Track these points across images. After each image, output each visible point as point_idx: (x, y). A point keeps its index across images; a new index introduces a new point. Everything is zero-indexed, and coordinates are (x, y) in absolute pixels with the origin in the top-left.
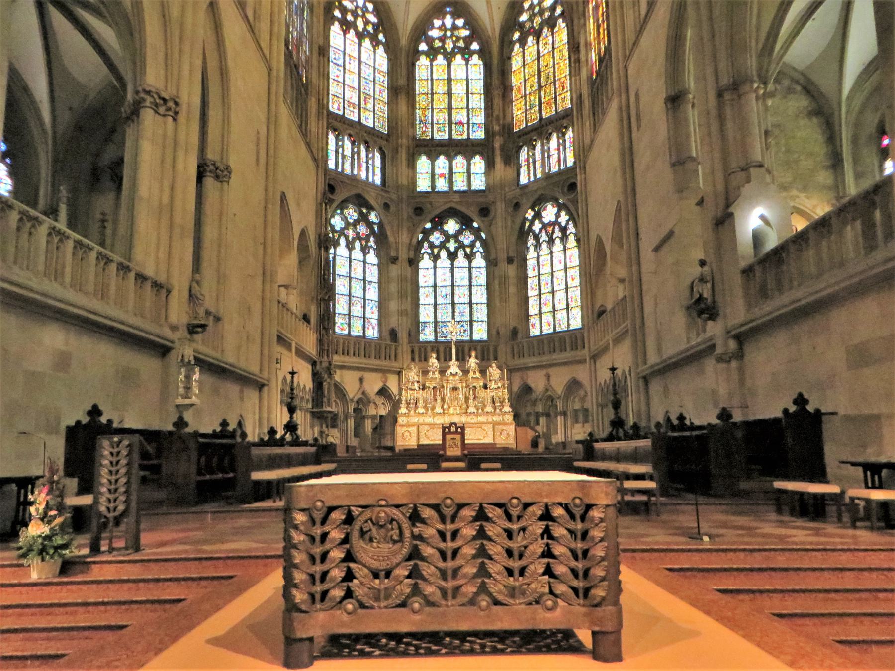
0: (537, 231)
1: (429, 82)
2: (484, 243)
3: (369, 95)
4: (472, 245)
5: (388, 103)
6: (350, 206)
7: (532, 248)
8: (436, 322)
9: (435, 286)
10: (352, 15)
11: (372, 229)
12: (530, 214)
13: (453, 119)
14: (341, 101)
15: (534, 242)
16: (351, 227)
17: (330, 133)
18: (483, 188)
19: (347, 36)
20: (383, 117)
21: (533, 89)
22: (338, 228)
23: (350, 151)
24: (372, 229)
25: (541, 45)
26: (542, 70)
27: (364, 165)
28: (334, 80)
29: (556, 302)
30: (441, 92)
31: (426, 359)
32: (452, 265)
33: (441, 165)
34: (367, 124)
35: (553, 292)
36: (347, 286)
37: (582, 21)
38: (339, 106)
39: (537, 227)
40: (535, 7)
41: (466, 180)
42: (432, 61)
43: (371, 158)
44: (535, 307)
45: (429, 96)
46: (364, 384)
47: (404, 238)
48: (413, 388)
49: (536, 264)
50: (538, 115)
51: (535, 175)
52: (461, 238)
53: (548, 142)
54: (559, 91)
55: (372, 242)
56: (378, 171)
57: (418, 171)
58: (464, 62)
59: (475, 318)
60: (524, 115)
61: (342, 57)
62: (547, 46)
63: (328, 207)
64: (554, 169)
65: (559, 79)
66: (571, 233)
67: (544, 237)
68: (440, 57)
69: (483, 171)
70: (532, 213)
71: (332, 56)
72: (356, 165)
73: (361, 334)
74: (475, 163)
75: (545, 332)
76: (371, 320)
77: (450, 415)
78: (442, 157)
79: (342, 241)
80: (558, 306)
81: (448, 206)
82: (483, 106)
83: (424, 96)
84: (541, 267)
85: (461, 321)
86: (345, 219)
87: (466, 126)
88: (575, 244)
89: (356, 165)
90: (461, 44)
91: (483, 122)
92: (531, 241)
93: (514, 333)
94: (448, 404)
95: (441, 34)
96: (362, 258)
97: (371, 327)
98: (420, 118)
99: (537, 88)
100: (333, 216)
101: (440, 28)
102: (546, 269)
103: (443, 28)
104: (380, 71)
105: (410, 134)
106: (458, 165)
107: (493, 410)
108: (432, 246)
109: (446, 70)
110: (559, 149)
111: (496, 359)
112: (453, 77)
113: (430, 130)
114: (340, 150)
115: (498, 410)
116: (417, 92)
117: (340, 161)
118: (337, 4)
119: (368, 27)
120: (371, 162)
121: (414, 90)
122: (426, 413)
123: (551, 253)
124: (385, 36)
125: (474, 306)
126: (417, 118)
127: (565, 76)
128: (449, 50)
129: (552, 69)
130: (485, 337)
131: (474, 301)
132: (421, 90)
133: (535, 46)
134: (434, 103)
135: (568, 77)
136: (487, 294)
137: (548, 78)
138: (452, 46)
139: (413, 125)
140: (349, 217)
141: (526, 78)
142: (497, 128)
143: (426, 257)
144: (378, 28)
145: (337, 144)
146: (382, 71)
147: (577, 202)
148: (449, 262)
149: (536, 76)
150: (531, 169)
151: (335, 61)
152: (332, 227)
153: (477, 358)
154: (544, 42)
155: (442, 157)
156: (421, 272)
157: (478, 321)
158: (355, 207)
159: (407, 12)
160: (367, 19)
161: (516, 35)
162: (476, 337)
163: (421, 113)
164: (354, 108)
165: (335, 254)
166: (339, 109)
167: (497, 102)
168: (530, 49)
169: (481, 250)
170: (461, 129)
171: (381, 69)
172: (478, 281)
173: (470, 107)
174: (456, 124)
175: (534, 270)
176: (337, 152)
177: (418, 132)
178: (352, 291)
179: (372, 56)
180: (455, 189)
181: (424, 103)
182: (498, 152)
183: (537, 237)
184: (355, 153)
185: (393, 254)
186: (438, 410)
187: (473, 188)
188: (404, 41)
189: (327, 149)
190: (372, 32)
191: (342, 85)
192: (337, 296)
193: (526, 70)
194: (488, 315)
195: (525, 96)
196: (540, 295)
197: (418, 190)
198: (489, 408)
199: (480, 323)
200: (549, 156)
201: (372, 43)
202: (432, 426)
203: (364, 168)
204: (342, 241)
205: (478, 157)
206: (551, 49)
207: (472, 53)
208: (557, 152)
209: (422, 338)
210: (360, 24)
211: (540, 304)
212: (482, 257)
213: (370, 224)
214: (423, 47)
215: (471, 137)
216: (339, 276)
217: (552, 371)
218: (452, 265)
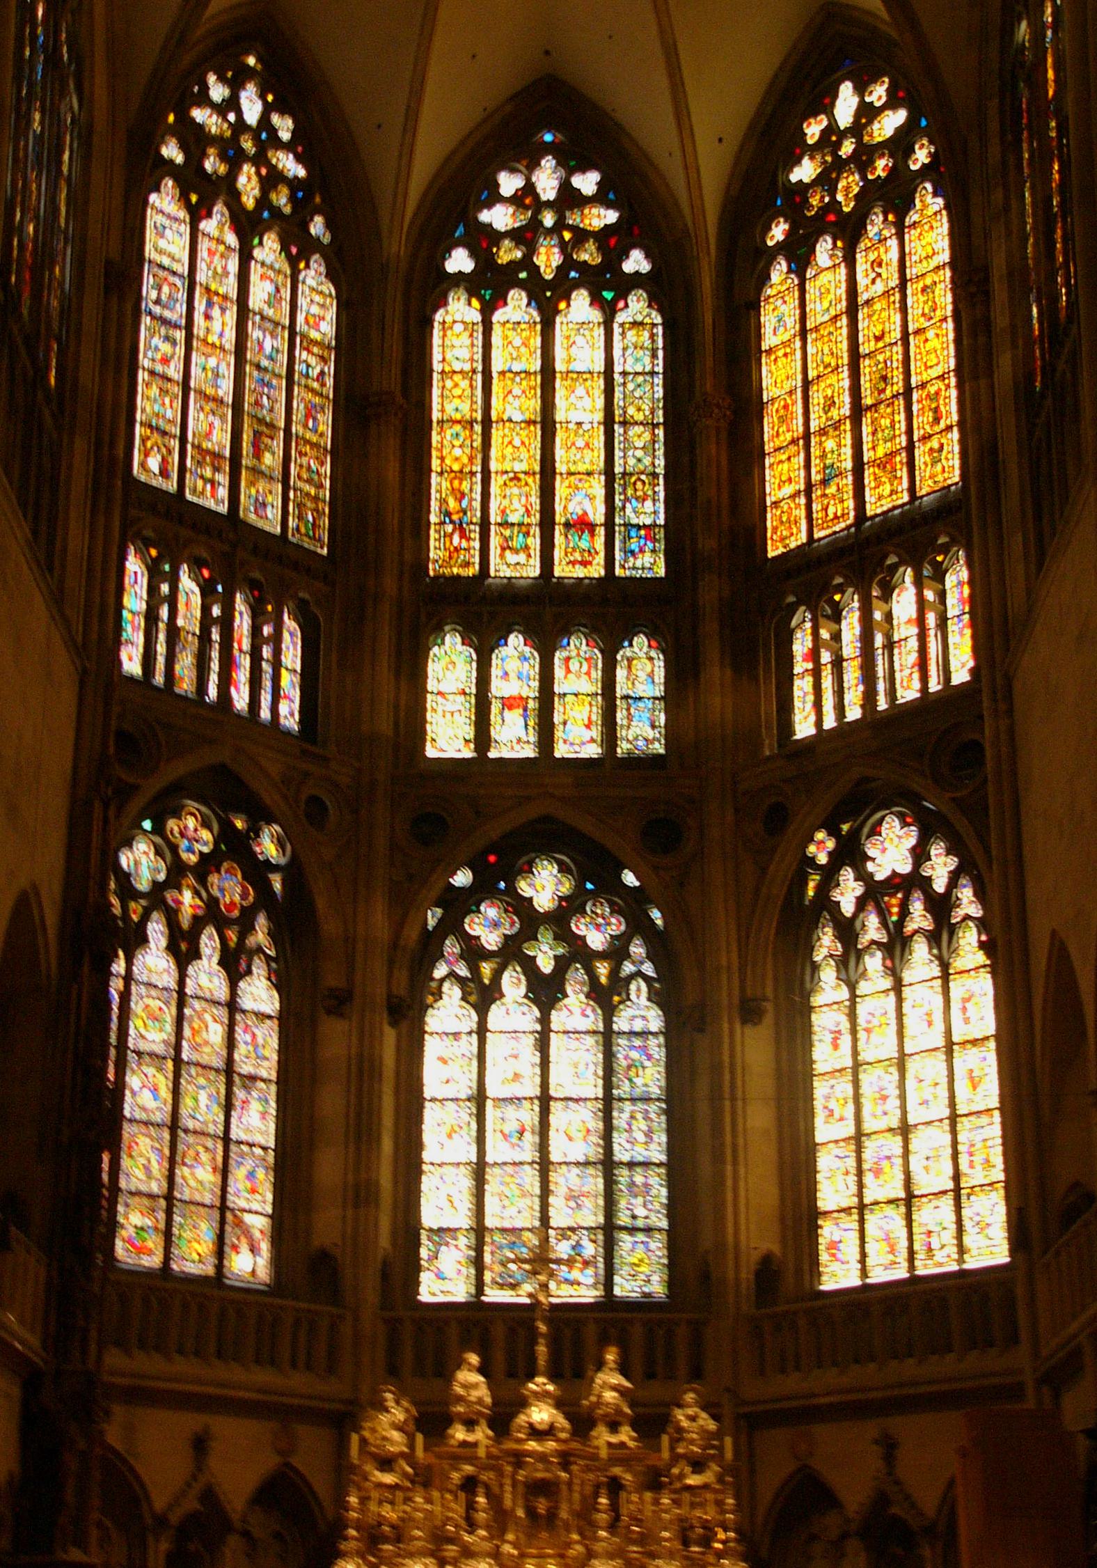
0: (848, 908)
1: (479, 377)
2: (659, 947)
3: (271, 426)
4: (616, 952)
5: (334, 453)
6: (192, 805)
7: (828, 974)
8: (480, 1231)
9: (479, 1099)
10: (223, 157)
11: (263, 888)
12: (821, 848)
13: (558, 508)
14: (175, 444)
15: (839, 949)
16: (191, 880)
17: (132, 550)
18: (659, 748)
19: (204, 225)
20: (316, 499)
21: (834, 413)
22: (143, 883)
23: (198, 614)
24: (263, 888)
25: (861, 266)
26: (864, 349)
27: (246, 662)
28: (152, 373)
29: (915, 1164)
30: (517, 417)
31: (445, 1372)
32: (545, 1020)
33: (513, 665)
34: (260, 524)
36: (165, 1093)
37: (998, 196)
38: (164, 461)
39: (848, 893)
40: (843, 135)
41: (596, 717)
42: (487, 311)
43: (267, 641)
44: (840, 1178)
45: (478, 428)
46: (214, 1463)
47: (379, 921)
49: (845, 1025)
50: (850, 504)
51: (840, 708)
52: (580, 927)
53: (887, 596)
54: (922, 422)
55: (260, 936)
56: (290, 683)
57: (431, 685)
58: (596, 316)
59: (623, 1219)
60: (802, 500)
61: (182, 296)
62: (882, 271)
63: (112, 813)
64: (908, 693)
65: (923, 386)
66: (967, 917)
67: (872, 930)
68: (517, 299)
69: (659, 691)
70: (831, 844)
71: (149, 292)
72: (215, 666)
73: (210, 1270)
74: (630, 660)
75: (878, 1276)
76: (248, 1219)
78: (516, 640)
79: (156, 930)
80: (923, 1184)
81: (533, 811)
82: (660, 470)
83: (458, 428)
84: (862, 1035)
86: (167, 849)
87: (601, 531)
88: (981, 958)
89: (215, 666)
90: (589, 255)
91: (661, 521)
92: (826, 942)
93: (767, 1272)
95: (523, 219)
96: (222, 993)
97: (244, 1248)
98: (443, 501)
99: (846, 410)
100: (128, 843)
101: (517, 200)
102: (879, 1045)
103: (526, 198)
104: (309, 344)
105: (408, 556)
106: (574, 665)
108: (473, 952)
109: (537, 341)
110: (921, 621)
111: (696, 1374)
112: (560, 366)
113: (477, 544)
114: (164, 612)
116: (436, 415)
117: (161, 648)
118: (171, 118)
119: (273, 196)
120: (266, 652)
121: (424, 406)
123: (898, 987)
124: (328, 225)
125: (623, 1175)
126: (434, 505)
127: (941, 377)
128: (549, 276)
129: (899, 349)
130: (657, 1288)
131: (621, 1154)
132: (449, 408)
133: (843, 271)
134: (494, 453)
135: (953, 381)
136: (670, 1132)
137: (884, 378)
138: (556, 259)
139: (420, 528)
140: (184, 844)
141: (812, 374)
142: (708, 544)
143: (452, 993)
144: (309, 197)
145: (152, 590)
146: (316, 343)
147: (986, 809)
148: (537, 1013)
149: (845, 374)
150: (827, 682)
151: (157, 310)
152: (125, 879)
153: (624, 1370)
154: (872, 256)
155: (516, 640)
156: (432, 1048)
157: (632, 1230)
158: (204, 809)
159: (407, 152)
160: (273, 169)
161: (778, 232)
162: (625, 1288)
163: (445, 485)
164: (216, 469)
165: (128, 978)
166: (164, 473)
167: (713, 452)
168: (825, 278)
169: (648, 969)
170: (584, 544)
171: (314, 335)
172: (639, 1081)
173: (618, 469)
174: (567, 525)
175: (836, 1046)
176: (151, 617)
177: (436, 552)
178: (184, 1112)
179: (286, 294)
180: (561, 751)
181: (457, 452)
182: (710, 627)
183: (847, 931)
184: (216, 621)
185: (332, 979)
187: (623, 748)
188: (396, 245)
189: (120, 606)
190: (287, 210)
191: (177, 390)
192: (126, 1125)
193: (811, 350)
194: (672, 1209)
195: (807, 436)
196: (858, 1139)
197: (431, 752)
199: (641, 1237)
200: (890, 646)
201: (285, 248)
203: (242, 676)
204: (156, 930)
205: (640, 641)
206: (894, 282)
207: (625, 285)
208: (914, 630)
209: (430, 1290)
210: (248, 183)
211: (860, 1173)
212: (655, 997)
213: (256, 871)
214: (460, 261)
215: (619, 572)
216: (139, 1053)
217: (898, 1424)
218: (545, 1020)
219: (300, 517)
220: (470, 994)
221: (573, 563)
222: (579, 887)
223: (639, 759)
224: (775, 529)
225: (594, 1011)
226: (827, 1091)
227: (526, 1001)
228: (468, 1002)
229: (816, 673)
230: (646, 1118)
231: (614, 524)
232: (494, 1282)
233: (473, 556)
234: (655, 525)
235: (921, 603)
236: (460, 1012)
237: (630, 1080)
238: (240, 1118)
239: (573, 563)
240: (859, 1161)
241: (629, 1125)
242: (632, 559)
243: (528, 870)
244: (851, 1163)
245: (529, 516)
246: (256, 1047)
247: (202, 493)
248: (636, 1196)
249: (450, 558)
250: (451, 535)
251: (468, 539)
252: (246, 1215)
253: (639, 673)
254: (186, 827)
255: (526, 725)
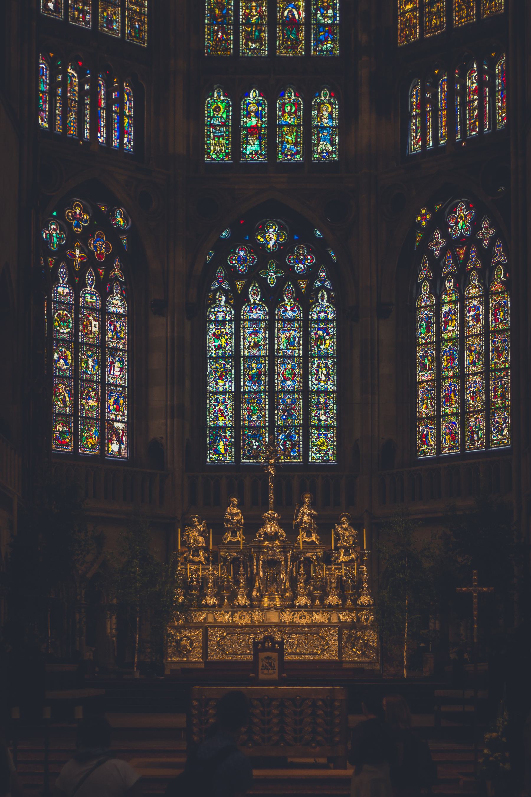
7: (425, 289)
24: (117, 244)
32: (271, 313)
35: (462, 377)
48: (196, 559)
67: (449, 266)
77: (263, 609)
85: (287, 427)
94: (259, 590)
107: (340, 602)
110: (479, 91)
115: (349, 603)
122: (220, 605)
123: (462, 299)
172: (322, 347)
174: (284, 25)
175: (428, 330)
186: (242, 600)
198: (333, 600)
202: (231, 628)
211: (438, 398)
219: (132, 26)
220: (231, 299)
221: (287, 48)
222: (290, 238)
223: (324, 163)
224: (402, 30)
225: (298, 308)
226: (422, 354)
227: (260, 303)
228: (229, 304)
229: (423, 115)
230: (326, 367)
231: (310, 24)
232: (244, 454)
233: (230, 44)
234: (333, 24)
235: (480, 81)
236: (224, 309)
237: (318, 347)
238: (110, 371)
239: (287, 48)
240: (439, 392)
241: (317, 371)
242: (320, 46)
243: (262, 230)
244: (434, 394)
245: (262, 20)
246: (117, 333)
247: (78, 18)
248: (320, 410)
249: (217, 45)
250: (217, 32)
251: (228, 34)
252: (115, 423)
253: (325, 113)
254: (75, 213)
255: (260, 145)
